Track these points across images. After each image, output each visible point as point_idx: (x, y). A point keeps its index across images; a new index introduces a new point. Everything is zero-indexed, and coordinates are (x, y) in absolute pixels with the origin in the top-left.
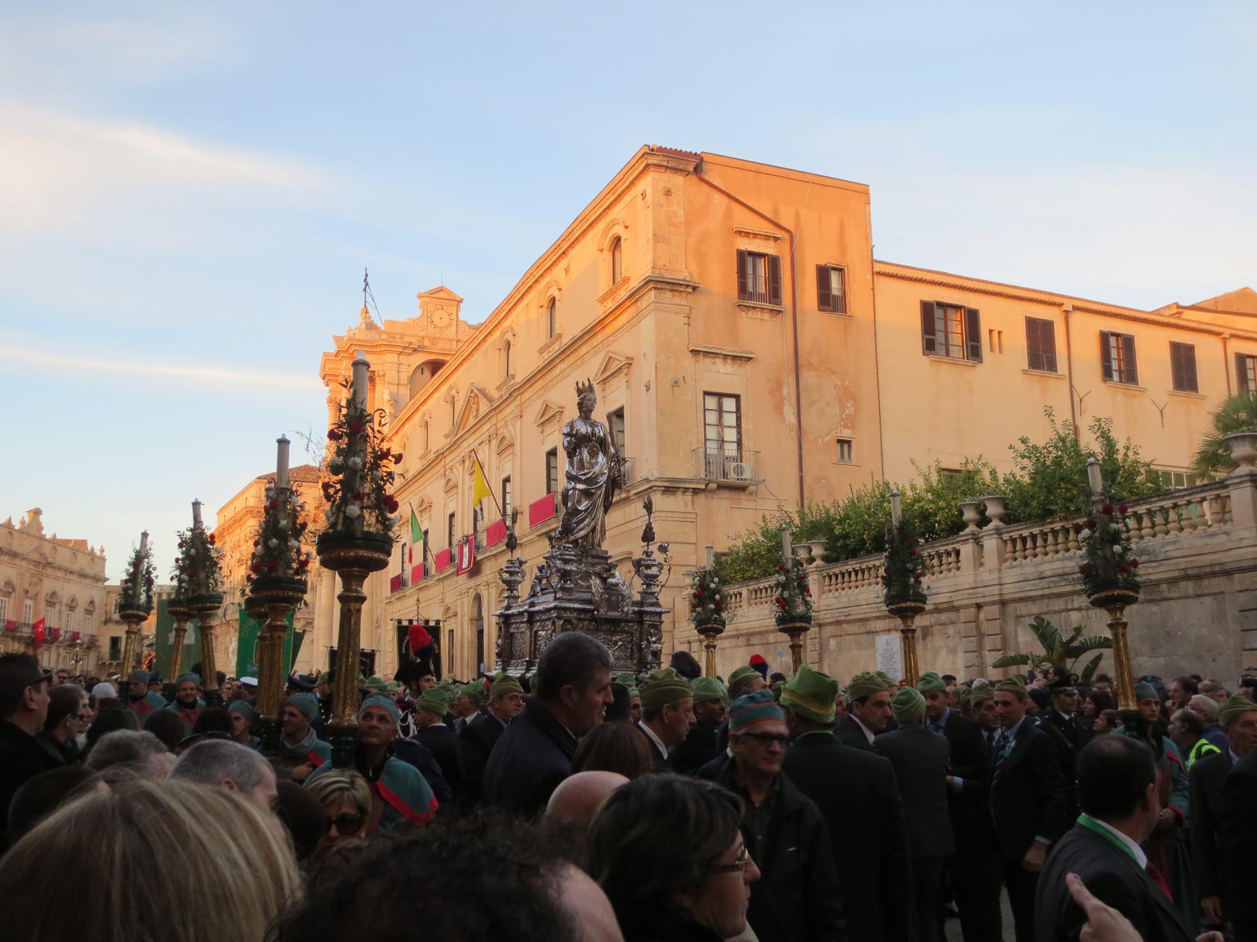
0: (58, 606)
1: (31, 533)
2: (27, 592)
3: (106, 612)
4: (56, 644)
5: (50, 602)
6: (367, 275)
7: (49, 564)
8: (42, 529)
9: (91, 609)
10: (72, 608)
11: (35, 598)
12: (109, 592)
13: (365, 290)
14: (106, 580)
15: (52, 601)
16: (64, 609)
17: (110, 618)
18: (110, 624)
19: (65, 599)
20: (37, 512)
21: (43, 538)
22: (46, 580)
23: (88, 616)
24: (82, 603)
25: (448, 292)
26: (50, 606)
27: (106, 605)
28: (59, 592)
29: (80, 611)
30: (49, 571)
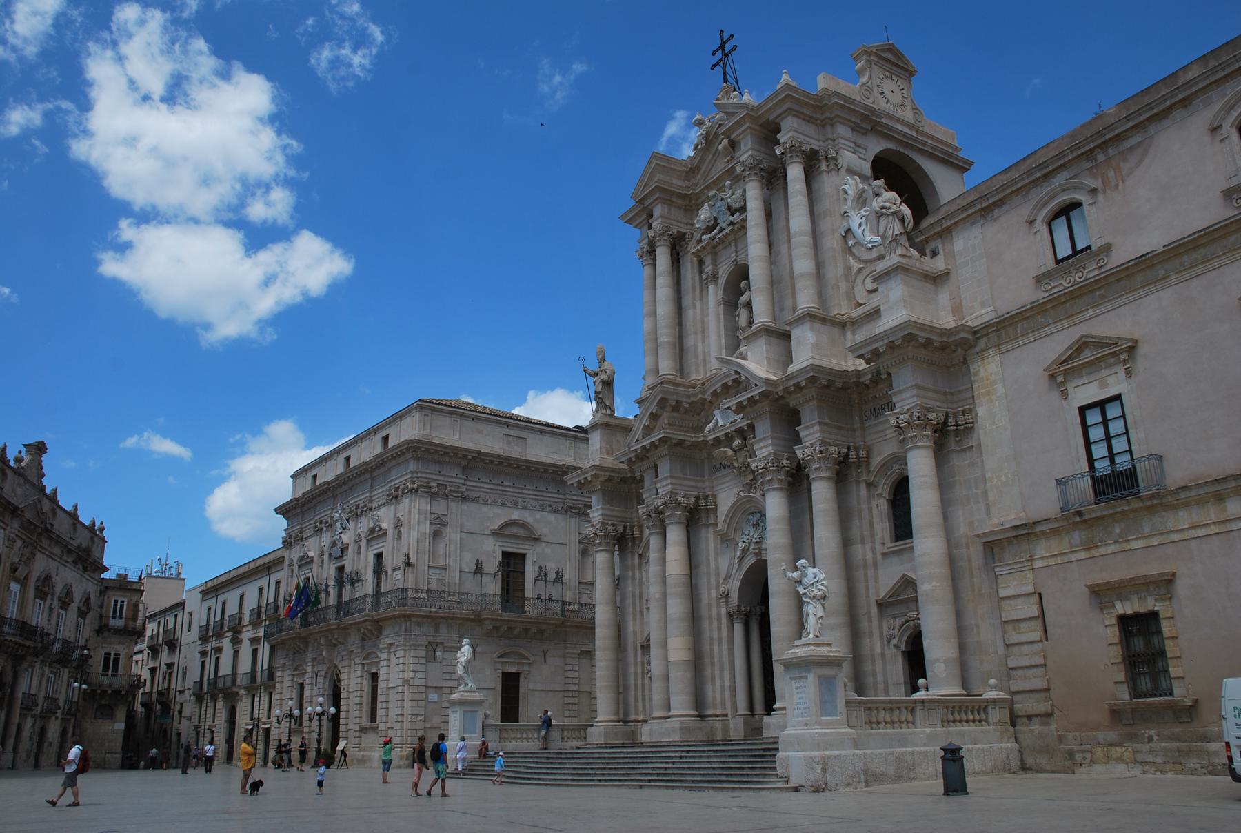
0: (49, 597)
1: (29, 478)
2: (16, 569)
3: (101, 616)
4: (41, 658)
5: (41, 591)
7: (47, 530)
8: (43, 475)
9: (84, 609)
10: (65, 605)
11: (23, 583)
12: (107, 588)
14: (106, 569)
15: (44, 587)
16: (56, 604)
17: (107, 625)
18: (106, 634)
19: (58, 589)
20: (39, 449)
21: (43, 489)
22: (39, 556)
23: (80, 620)
24: (77, 596)
25: (899, 55)
26: (40, 598)
27: (101, 606)
28: (56, 579)
29: (73, 608)
30: (45, 542)
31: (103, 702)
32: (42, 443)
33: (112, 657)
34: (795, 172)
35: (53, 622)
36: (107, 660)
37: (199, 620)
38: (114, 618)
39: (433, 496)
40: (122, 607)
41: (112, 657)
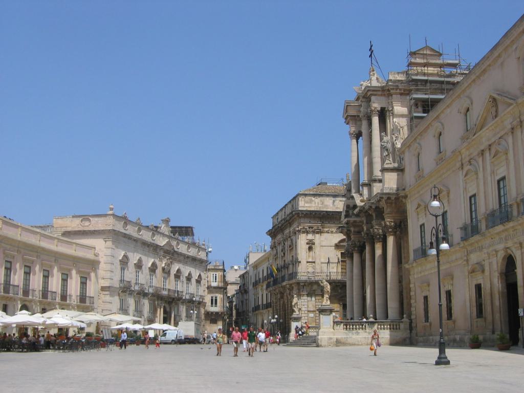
0: (181, 277)
6: (371, 46)
7: (175, 251)
13: (371, 56)
16: (185, 280)
24: (195, 276)
28: (182, 269)
31: (213, 317)
32: (168, 218)
33: (214, 298)
34: (376, 120)
35: (185, 285)
36: (212, 300)
37: (253, 280)
38: (213, 282)
39: (307, 233)
40: (216, 277)
41: (214, 298)
